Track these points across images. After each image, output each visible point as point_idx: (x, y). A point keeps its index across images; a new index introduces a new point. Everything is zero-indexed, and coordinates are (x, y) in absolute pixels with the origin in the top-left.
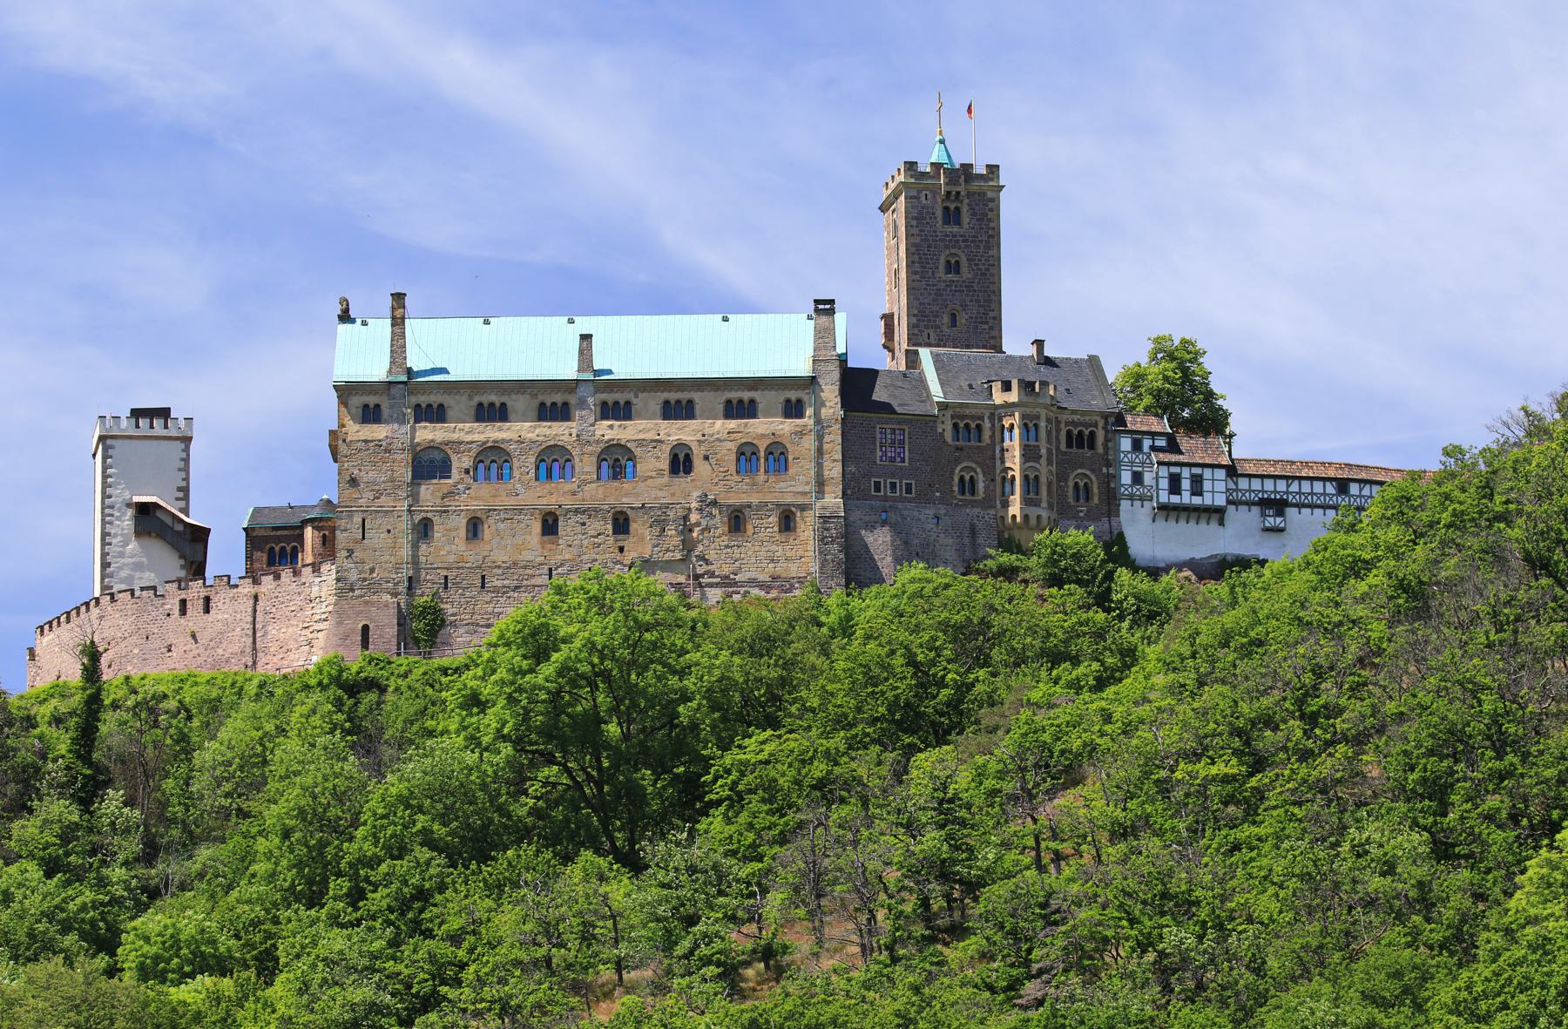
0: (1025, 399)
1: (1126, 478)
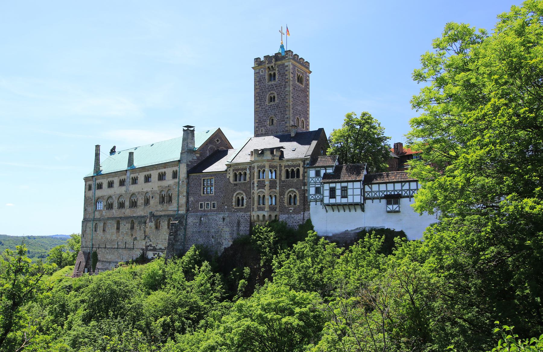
0: (257, 159)
1: (312, 191)
